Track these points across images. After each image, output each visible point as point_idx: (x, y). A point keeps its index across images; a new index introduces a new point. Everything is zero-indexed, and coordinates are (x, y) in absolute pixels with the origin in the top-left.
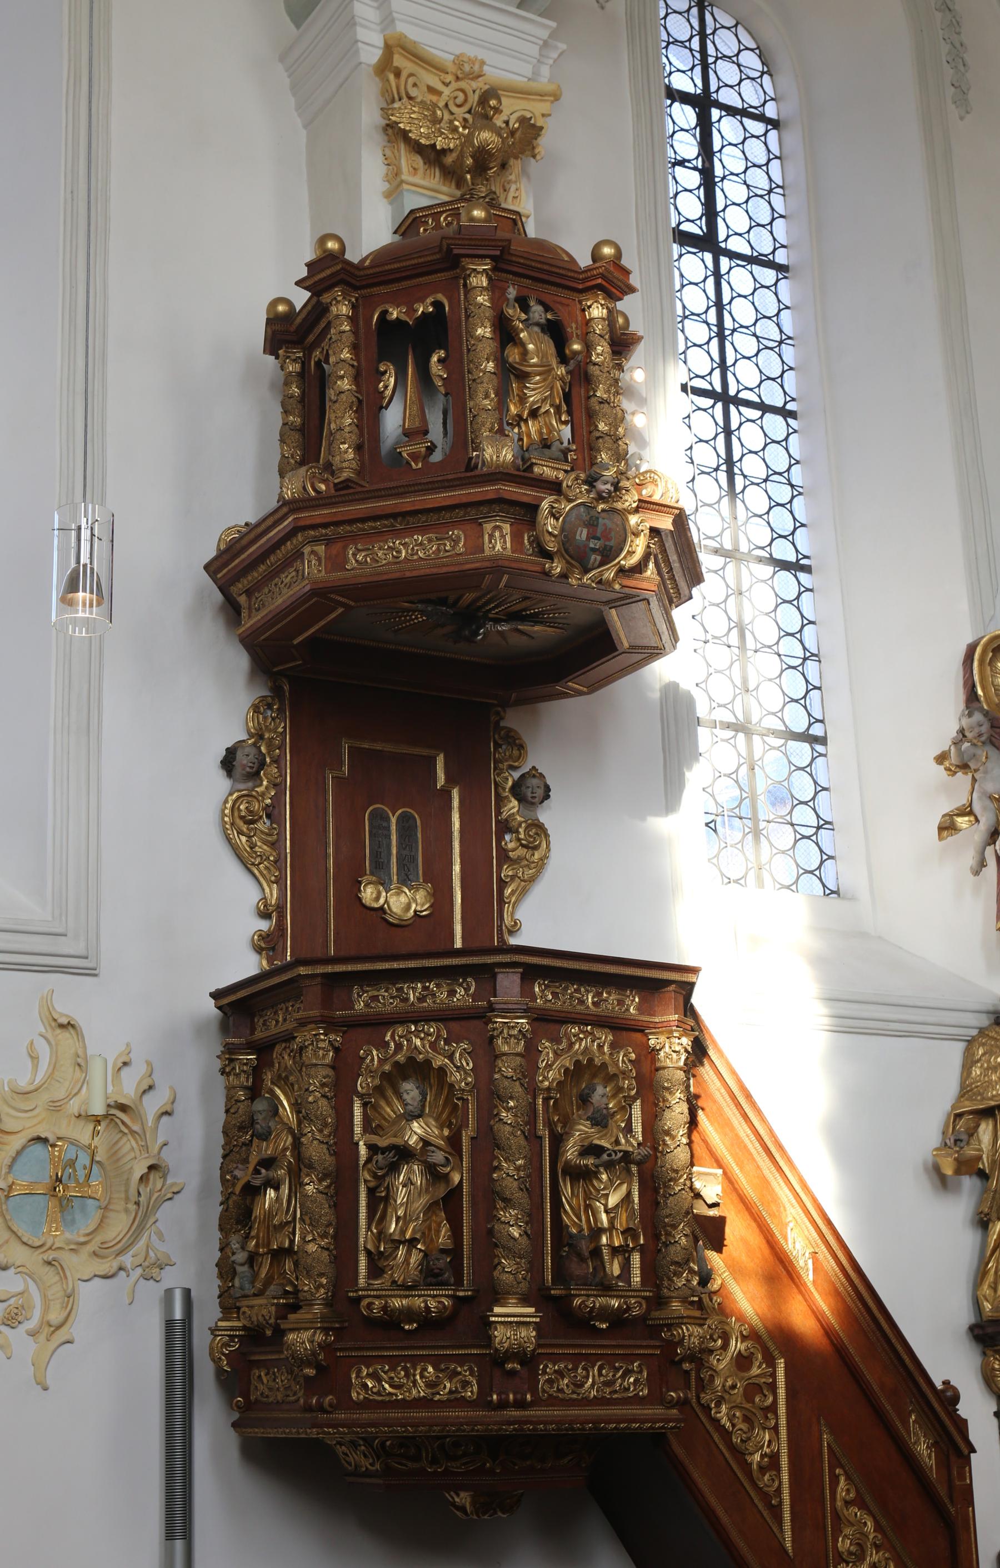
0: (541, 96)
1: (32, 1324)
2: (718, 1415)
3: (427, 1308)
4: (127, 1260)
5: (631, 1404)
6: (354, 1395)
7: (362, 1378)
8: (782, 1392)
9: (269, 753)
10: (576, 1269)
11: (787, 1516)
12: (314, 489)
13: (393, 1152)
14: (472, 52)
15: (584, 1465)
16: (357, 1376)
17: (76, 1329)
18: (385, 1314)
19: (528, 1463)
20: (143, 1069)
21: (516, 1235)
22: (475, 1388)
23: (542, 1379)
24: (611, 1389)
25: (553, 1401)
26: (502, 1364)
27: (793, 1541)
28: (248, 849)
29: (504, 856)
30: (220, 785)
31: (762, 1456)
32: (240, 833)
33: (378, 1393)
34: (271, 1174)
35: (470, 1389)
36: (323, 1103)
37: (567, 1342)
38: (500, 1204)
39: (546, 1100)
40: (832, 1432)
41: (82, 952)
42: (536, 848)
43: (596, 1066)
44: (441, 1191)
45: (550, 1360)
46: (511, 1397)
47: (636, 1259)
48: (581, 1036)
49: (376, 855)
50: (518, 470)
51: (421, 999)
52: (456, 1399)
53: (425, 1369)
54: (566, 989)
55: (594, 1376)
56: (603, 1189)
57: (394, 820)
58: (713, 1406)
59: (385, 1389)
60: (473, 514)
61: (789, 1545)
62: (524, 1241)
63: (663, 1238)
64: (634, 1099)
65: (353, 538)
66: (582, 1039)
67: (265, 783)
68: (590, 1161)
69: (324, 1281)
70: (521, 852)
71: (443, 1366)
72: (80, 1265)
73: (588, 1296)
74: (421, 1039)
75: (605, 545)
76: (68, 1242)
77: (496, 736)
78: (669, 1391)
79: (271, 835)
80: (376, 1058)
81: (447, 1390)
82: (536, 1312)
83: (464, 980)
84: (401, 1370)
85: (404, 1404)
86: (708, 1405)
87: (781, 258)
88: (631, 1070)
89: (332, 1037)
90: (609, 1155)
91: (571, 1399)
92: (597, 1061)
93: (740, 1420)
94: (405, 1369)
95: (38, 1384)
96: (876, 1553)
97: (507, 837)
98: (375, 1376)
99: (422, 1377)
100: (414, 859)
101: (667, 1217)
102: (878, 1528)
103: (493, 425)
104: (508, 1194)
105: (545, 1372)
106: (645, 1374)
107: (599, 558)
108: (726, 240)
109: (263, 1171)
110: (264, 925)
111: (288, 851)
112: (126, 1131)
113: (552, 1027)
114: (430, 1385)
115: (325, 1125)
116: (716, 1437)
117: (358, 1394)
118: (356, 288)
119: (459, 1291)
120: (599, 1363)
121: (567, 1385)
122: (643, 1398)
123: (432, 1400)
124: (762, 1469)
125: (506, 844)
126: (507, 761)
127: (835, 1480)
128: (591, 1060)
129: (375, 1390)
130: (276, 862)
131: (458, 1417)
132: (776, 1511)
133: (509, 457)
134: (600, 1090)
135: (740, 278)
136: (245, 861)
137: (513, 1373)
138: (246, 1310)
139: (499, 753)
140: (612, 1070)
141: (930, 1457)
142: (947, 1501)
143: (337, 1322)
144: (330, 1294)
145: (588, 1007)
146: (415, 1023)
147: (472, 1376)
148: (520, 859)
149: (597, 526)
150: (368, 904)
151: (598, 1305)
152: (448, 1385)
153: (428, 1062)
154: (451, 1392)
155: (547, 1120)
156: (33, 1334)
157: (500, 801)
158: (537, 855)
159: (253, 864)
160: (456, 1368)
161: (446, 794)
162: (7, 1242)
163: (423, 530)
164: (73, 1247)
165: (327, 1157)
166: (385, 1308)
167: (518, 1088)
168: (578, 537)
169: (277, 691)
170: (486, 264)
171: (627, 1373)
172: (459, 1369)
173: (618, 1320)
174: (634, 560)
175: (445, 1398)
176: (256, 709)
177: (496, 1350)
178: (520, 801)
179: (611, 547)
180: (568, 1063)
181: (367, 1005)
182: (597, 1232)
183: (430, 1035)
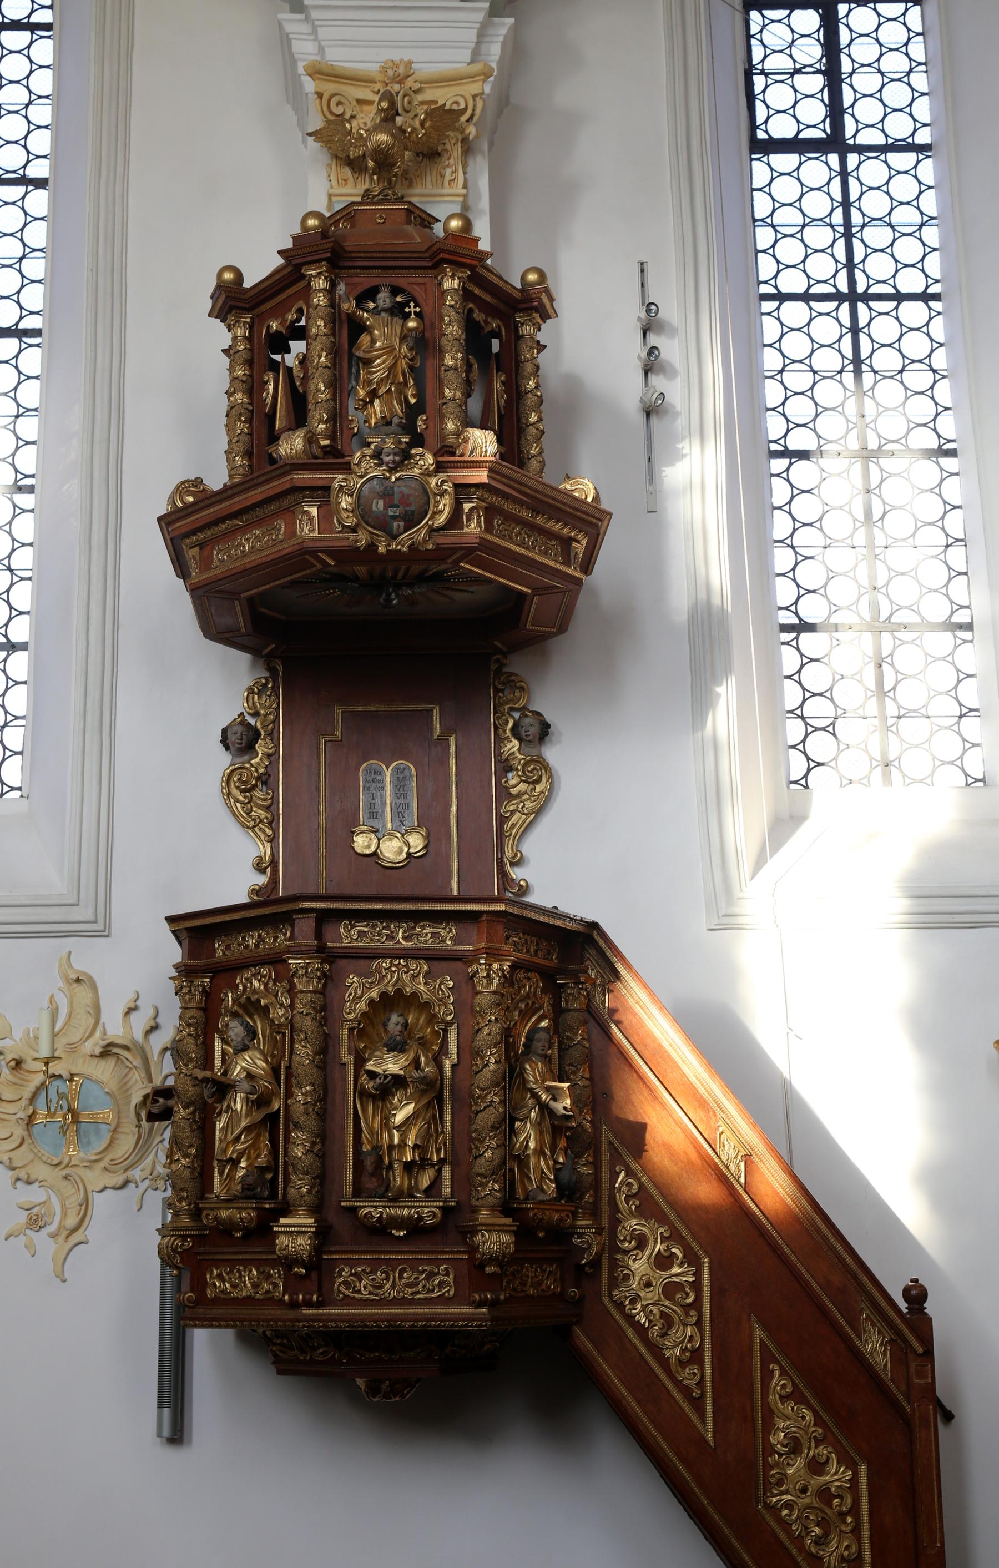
0: (472, 77)
1: (52, 1228)
2: (634, 1311)
4: (136, 1174)
5: (436, 1304)
8: (706, 1290)
9: (263, 728)
10: (370, 1183)
11: (709, 1408)
12: (182, 501)
14: (397, 55)
17: (92, 1231)
20: (151, 1013)
21: (300, 1154)
25: (348, 1301)
26: (290, 1268)
27: (715, 1433)
28: (244, 815)
29: (505, 794)
30: (224, 760)
31: (683, 1351)
40: (765, 1327)
41: (92, 918)
42: (538, 781)
44: (258, 1116)
46: (301, 1297)
47: (447, 1171)
49: (371, 806)
50: (315, 457)
51: (257, 946)
53: (250, 1272)
54: (374, 927)
55: (394, 1277)
56: (393, 1110)
57: (388, 774)
58: (627, 1303)
60: (286, 502)
61: (710, 1436)
64: (450, 1023)
65: (215, 540)
66: (394, 972)
67: (260, 755)
70: (523, 787)
72: (95, 1178)
73: (376, 1207)
74: (259, 981)
75: (406, 511)
76: (82, 1160)
77: (496, 683)
79: (265, 800)
80: (230, 999)
82: (315, 1222)
85: (235, 1301)
86: (622, 1302)
87: (923, 137)
88: (449, 997)
89: (197, 982)
91: (367, 1300)
93: (658, 1317)
94: (239, 1271)
95: (57, 1277)
96: (816, 1447)
98: (220, 1277)
100: (407, 806)
102: (818, 1421)
103: (321, 415)
105: (341, 1276)
106: (452, 1276)
107: (402, 524)
108: (854, 136)
109: (161, 1100)
110: (262, 880)
111: (281, 812)
112: (131, 1066)
113: (363, 963)
114: (255, 1286)
116: (630, 1332)
118: (248, 310)
119: (266, 1203)
121: (365, 1287)
122: (449, 1299)
123: (254, 1298)
124: (682, 1364)
125: (506, 782)
126: (507, 704)
127: (767, 1376)
128: (399, 992)
130: (270, 823)
132: (698, 1404)
133: (300, 446)
135: (873, 171)
136: (250, 825)
137: (301, 1277)
139: (500, 698)
141: (885, 1355)
142: (901, 1398)
143: (196, 1230)
144: (193, 1206)
145: (399, 942)
146: (255, 966)
148: (520, 795)
149: (393, 494)
150: (359, 851)
151: (385, 1216)
153: (258, 1001)
155: (353, 1048)
156: (53, 1236)
157: (500, 740)
158: (539, 788)
160: (269, 1271)
161: (443, 741)
162: (32, 1161)
163: (258, 523)
164: (86, 1164)
165: (191, 1089)
168: (374, 508)
169: (272, 670)
170: (321, 267)
171: (431, 1276)
173: (416, 1228)
174: (441, 520)
176: (250, 691)
178: (520, 740)
179: (413, 512)
180: (374, 994)
181: (224, 953)
182: (391, 1147)
183: (264, 977)
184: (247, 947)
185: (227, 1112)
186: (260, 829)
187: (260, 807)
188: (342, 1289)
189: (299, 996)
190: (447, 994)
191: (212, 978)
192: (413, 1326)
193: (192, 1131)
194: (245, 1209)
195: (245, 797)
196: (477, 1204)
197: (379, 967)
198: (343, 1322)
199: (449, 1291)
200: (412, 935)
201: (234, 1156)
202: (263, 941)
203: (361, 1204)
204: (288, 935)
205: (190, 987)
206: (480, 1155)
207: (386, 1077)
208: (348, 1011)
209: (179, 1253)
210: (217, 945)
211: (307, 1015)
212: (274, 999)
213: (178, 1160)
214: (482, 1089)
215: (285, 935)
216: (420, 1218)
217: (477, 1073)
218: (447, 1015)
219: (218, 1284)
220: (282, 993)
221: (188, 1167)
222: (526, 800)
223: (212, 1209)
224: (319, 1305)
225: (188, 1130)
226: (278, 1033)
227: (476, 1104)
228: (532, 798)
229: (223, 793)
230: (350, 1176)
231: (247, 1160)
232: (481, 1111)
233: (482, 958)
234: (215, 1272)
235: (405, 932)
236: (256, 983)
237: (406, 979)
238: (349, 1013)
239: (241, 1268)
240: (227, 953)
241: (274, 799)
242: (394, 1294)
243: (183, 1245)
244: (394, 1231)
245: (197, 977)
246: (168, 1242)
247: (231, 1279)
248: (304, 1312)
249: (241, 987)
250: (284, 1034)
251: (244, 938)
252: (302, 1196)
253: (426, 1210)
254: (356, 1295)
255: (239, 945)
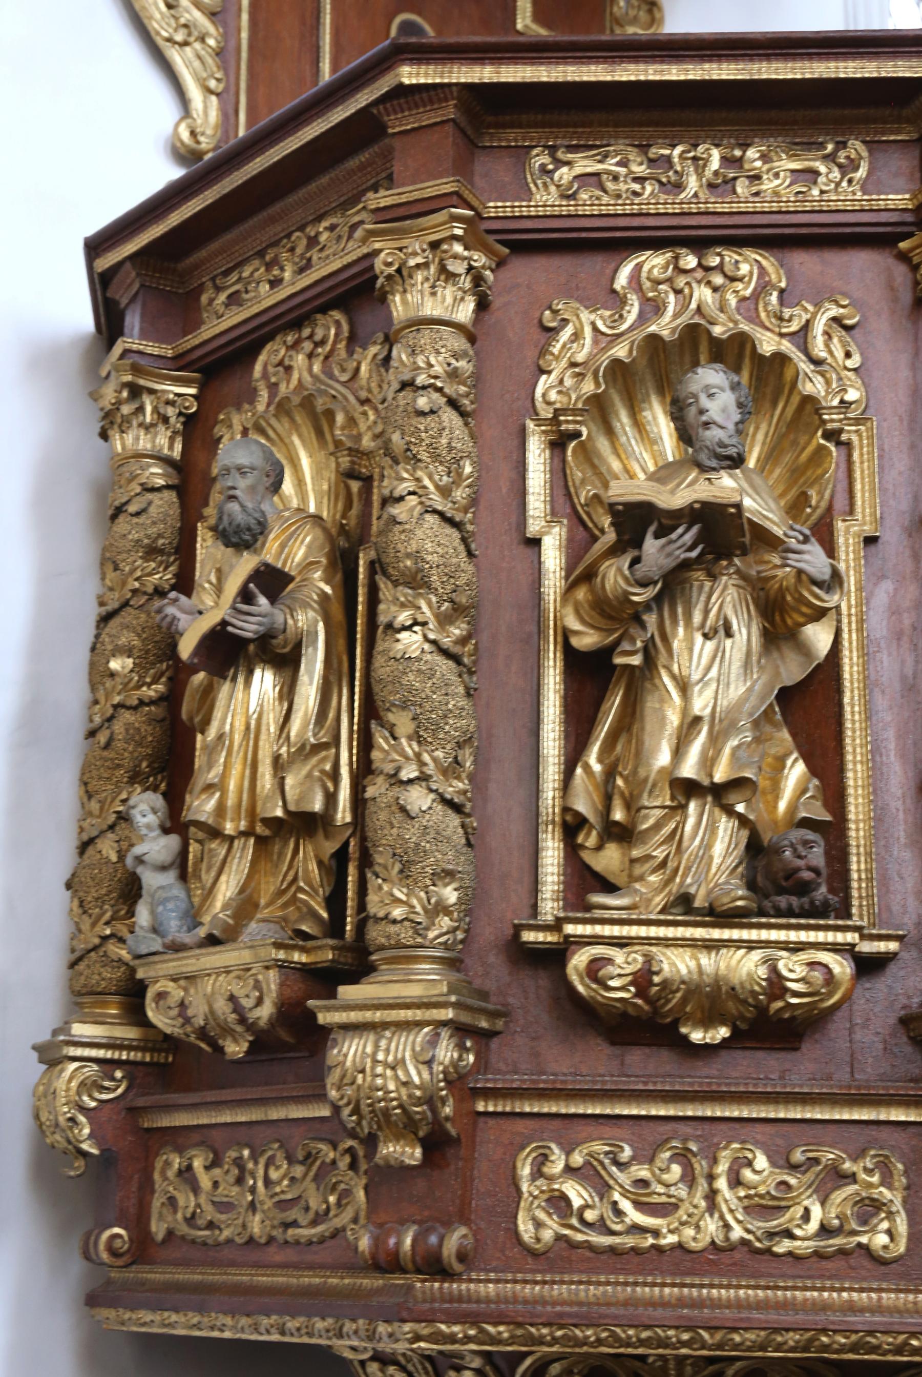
6: (525, 1228)
7: (551, 1179)
13: (695, 529)
16: (538, 1173)
22: (902, 1225)
33: (602, 1226)
35: (885, 1225)
52: (842, 1252)
59: (619, 1213)
69: (450, 895)
71: (798, 1156)
81: (813, 1226)
84: (672, 1159)
94: (683, 1157)
99: (736, 1182)
117: (538, 1225)
131: (851, 1308)
138: (170, 986)
146: (700, 245)
147: (890, 1187)
154: (825, 1230)
172: (847, 1165)
223: (621, 943)
236: (703, 294)
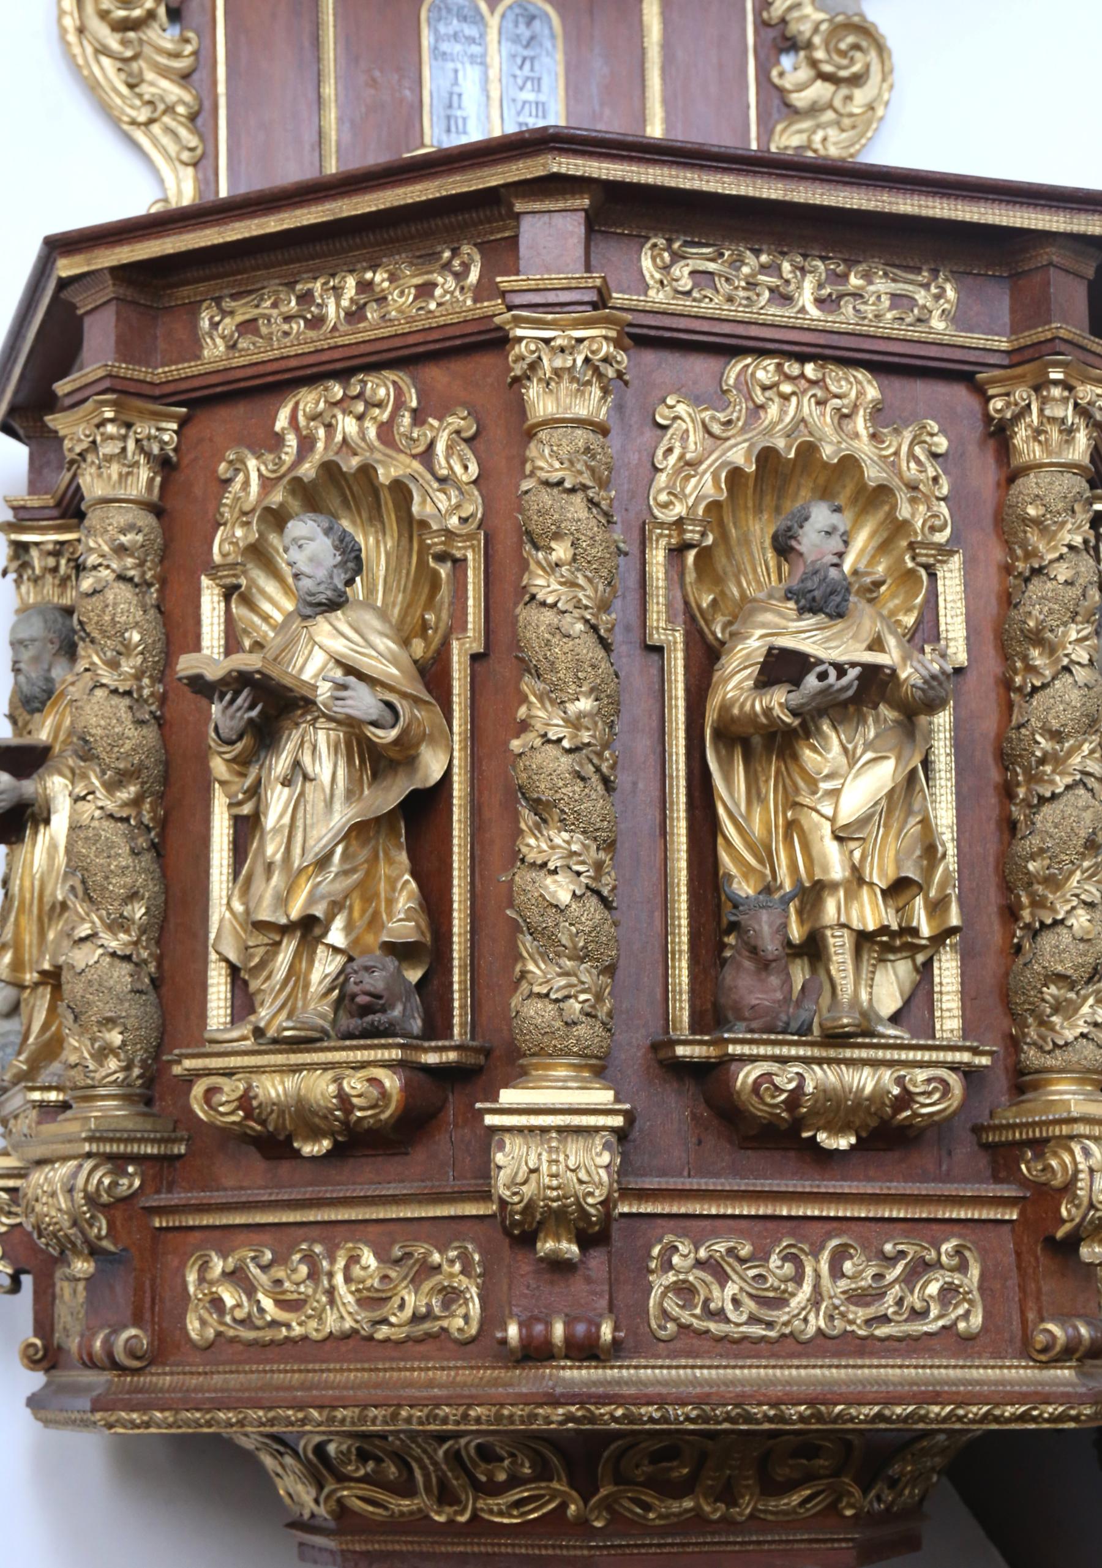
3: (343, 1098)
5: (933, 1353)
6: (193, 1326)
7: (211, 1283)
15: (849, 1513)
16: (202, 1280)
18: (248, 1116)
19: (688, 1504)
21: (564, 897)
22: (475, 1308)
23: (661, 1281)
24: (871, 1311)
26: (526, 1239)
28: (124, 90)
32: (102, 50)
34: (28, 787)
35: (462, 1311)
36: (122, 594)
37: (742, 1185)
38: (527, 818)
39: (677, 552)
42: (856, 80)
43: (825, 465)
45: (684, 1234)
48: (786, 388)
51: (355, 315)
52: (429, 1336)
53: (354, 1259)
54: (738, 262)
55: (818, 1275)
56: (829, 777)
59: (262, 1311)
62: (591, 912)
63: (1026, 914)
64: (945, 551)
66: (786, 398)
68: (777, 698)
70: (820, 90)
71: (397, 1252)
73: (783, 1060)
74: (360, 418)
78: (1042, 1320)
79: (177, 55)
81: (408, 1312)
82: (617, 1100)
83: (455, 252)
84: (301, 1261)
88: (935, 479)
89: (143, 429)
90: (822, 677)
91: (745, 1338)
92: (828, 452)
94: (309, 1259)
97: (787, 61)
98: (236, 1276)
99: (348, 1279)
101: (1033, 857)
104: (543, 790)
105: (668, 1266)
106: (975, 1272)
111: (222, 88)
113: (700, 366)
114: (371, 1300)
115: (126, 649)
117: (203, 1323)
119: (426, 1050)
120: (834, 1242)
121: (735, 1301)
122: (969, 1338)
123: (370, 1338)
125: (781, 74)
128: (809, 451)
129: (240, 1314)
130: (193, 117)
134: (821, 516)
137: (559, 1266)
140: (873, 474)
143: (153, 1141)
144: (136, 1072)
145: (803, 310)
146: (343, 375)
147: (468, 1275)
148: (814, 110)
151: (809, 1088)
152: (410, 1299)
153: (367, 471)
154: (416, 1318)
155: (680, 606)
158: (861, 96)
159: (133, 122)
160: (429, 1254)
165: (131, 731)
166: (245, 1101)
167: (577, 508)
171: (919, 1269)
172: (436, 1257)
175: (400, 1334)
177: (503, 1203)
180: (739, 455)
183: (379, 405)
184: (317, 322)
185: (287, 782)
186: (168, 130)
187: (164, 72)
188: (672, 1305)
189: (543, 435)
190: (931, 473)
191: (183, 422)
192: (879, 1417)
193: (135, 853)
194: (363, 1065)
195: (124, 43)
196: (1050, 1062)
197: (745, 385)
198: (684, 1404)
199: (966, 1316)
200: (841, 296)
201: (319, 911)
202: (382, 300)
203: (746, 1050)
204: (474, 276)
205: (124, 438)
206: (1056, 923)
207: (841, 669)
208: (663, 497)
209: (105, 1208)
210: (205, 324)
211: (572, 490)
212: (416, 465)
213: (92, 937)
214: (1057, 736)
215: (460, 276)
216: (906, 1099)
217: (1035, 690)
218: (933, 529)
219: (229, 1300)
220: (449, 448)
221: (127, 958)
222: (829, 124)
223: (229, 1073)
224: (617, 1350)
225: (124, 850)
226: (441, 558)
227: (1038, 779)
228: (846, 122)
229: (63, 31)
230: (682, 973)
231: (349, 928)
232: (1054, 797)
233: (1056, 364)
234: (218, 1266)
235: (820, 286)
236: (347, 425)
237: (823, 421)
238: (666, 506)
239: (318, 1249)
240: (243, 344)
241: (204, 58)
242: (817, 1322)
243: (114, 1184)
244: (822, 1137)
245: (143, 414)
246: (75, 1175)
247: (278, 1282)
248: (567, 1373)
249: (292, 440)
250: (459, 563)
251: (306, 298)
252: (570, 1024)
253: (921, 1075)
254: (713, 1326)
255: (288, 319)
